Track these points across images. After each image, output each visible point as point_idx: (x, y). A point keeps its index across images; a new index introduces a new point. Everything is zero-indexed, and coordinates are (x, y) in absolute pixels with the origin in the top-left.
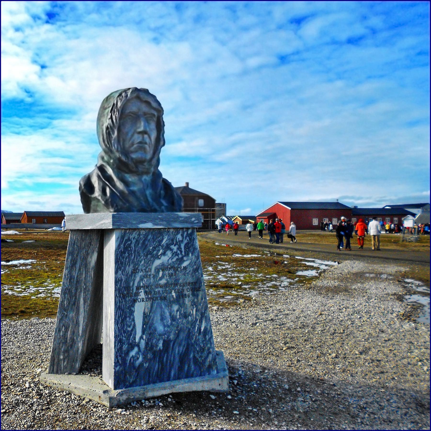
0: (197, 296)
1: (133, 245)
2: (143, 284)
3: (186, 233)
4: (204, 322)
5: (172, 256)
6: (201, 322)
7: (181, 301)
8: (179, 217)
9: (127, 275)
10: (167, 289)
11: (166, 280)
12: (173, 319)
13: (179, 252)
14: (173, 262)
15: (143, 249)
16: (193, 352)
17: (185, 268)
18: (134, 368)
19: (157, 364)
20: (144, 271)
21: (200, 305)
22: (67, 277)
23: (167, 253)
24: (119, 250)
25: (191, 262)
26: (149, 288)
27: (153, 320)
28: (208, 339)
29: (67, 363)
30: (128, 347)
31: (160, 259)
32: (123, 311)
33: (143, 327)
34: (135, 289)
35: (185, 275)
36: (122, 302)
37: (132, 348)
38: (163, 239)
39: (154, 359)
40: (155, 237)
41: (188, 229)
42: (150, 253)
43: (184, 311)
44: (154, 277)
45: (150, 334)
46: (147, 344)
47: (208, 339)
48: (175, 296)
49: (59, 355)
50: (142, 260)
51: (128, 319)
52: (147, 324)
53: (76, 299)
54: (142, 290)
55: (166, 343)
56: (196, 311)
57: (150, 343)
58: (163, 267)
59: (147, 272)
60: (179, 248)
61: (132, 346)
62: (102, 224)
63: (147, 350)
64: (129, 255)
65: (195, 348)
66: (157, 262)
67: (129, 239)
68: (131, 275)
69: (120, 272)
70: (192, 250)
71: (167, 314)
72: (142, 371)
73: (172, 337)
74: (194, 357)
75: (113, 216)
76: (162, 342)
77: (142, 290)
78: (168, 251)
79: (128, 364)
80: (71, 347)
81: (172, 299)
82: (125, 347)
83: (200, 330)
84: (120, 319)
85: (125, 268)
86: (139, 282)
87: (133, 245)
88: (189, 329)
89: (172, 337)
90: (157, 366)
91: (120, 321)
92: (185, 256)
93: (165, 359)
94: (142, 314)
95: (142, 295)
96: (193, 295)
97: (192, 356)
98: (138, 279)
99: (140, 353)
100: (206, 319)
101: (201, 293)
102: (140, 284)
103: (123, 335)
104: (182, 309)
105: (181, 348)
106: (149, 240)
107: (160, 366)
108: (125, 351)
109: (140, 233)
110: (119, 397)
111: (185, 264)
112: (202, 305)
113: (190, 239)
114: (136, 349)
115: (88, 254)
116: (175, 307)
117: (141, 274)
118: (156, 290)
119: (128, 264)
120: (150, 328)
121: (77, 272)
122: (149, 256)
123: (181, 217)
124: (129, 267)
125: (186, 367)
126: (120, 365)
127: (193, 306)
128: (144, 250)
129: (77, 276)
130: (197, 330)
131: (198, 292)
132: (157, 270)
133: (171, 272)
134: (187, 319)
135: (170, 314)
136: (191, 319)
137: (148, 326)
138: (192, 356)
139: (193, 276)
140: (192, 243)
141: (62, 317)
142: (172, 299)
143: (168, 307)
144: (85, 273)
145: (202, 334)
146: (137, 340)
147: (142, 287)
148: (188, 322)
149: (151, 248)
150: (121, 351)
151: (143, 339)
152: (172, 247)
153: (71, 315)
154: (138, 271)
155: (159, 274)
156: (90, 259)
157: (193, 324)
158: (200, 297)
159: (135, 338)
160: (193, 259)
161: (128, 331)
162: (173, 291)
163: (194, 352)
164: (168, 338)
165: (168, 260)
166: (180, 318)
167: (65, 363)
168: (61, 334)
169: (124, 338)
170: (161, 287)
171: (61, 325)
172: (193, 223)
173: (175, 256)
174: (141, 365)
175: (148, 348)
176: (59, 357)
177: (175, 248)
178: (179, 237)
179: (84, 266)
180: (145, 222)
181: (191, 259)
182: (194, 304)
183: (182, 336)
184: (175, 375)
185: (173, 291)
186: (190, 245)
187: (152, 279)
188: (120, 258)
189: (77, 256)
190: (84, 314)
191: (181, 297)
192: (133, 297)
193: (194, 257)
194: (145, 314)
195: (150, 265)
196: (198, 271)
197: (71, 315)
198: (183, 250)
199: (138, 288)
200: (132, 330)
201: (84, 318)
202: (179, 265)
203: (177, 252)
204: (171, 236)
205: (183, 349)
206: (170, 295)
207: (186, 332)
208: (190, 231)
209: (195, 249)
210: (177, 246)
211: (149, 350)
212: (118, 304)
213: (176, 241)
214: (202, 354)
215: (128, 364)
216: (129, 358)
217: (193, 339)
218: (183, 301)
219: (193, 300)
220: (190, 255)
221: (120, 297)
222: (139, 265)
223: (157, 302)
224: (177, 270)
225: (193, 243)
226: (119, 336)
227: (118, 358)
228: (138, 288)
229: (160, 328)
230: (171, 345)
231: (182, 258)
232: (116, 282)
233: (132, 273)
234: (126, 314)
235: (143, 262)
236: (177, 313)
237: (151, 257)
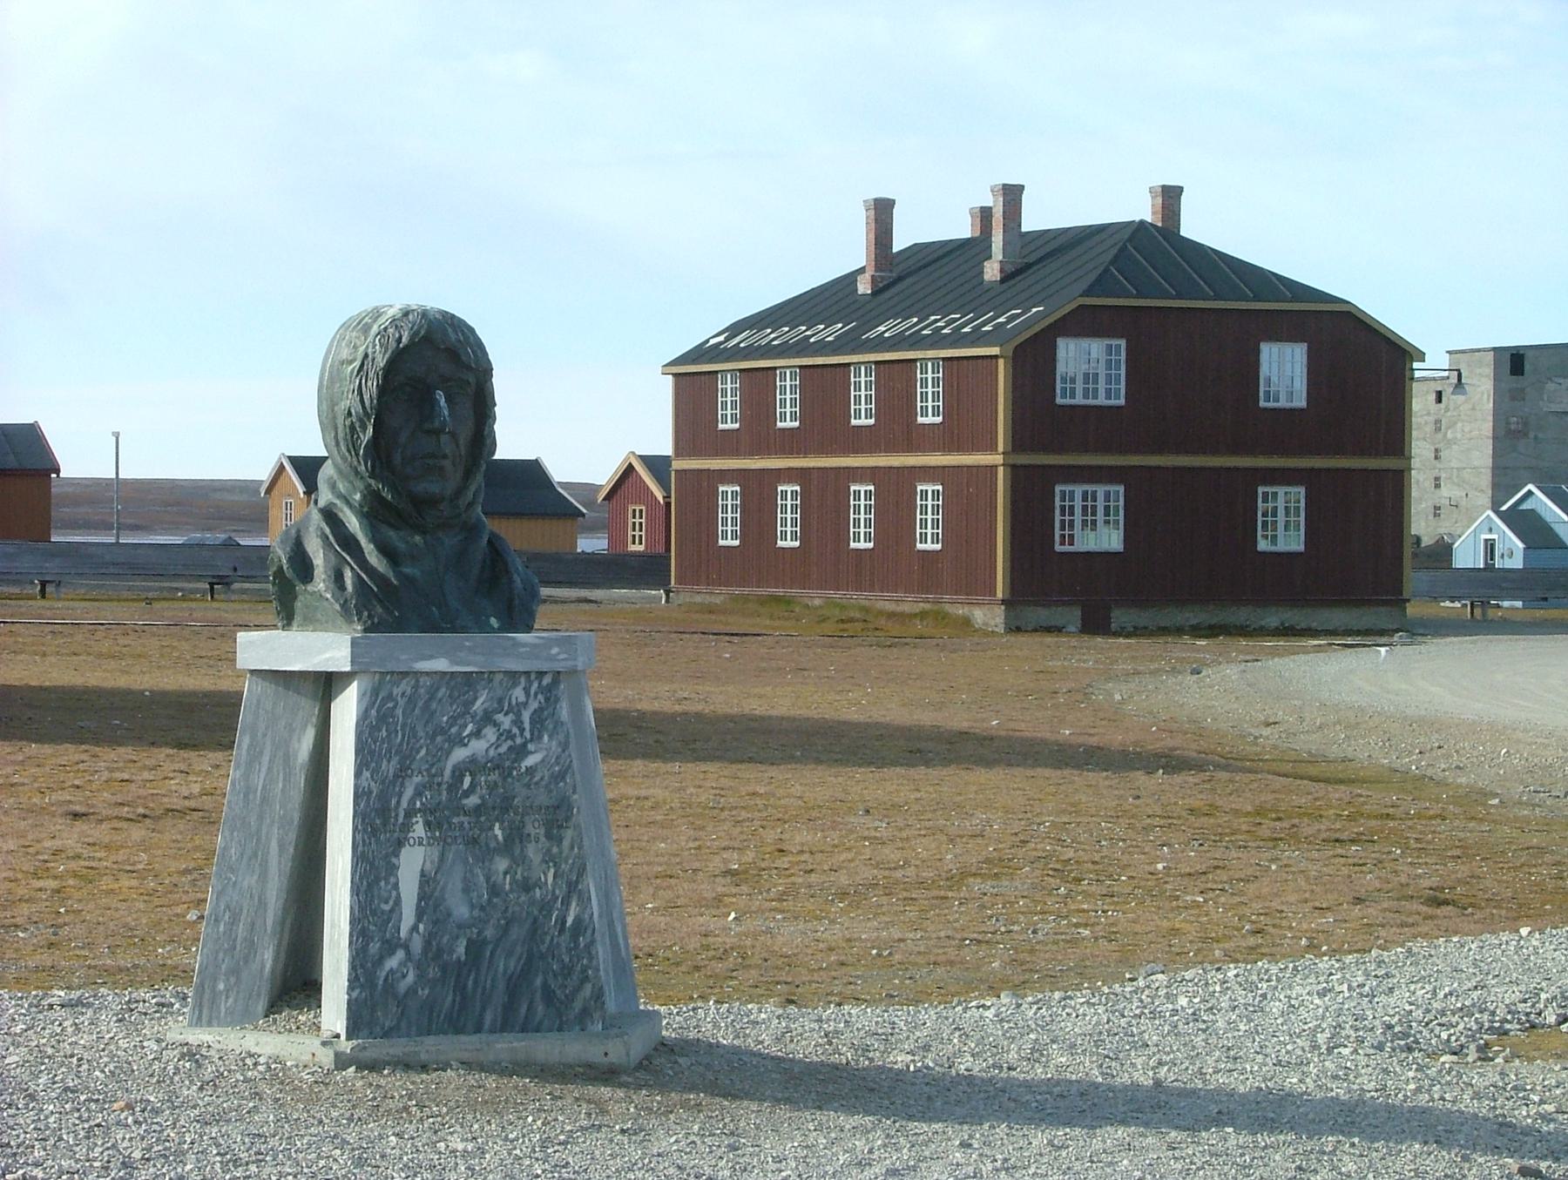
0: (561, 840)
1: (399, 712)
3: (535, 685)
4: (574, 904)
6: (566, 903)
7: (517, 852)
8: (516, 644)
9: (383, 782)
12: (494, 890)
13: (515, 730)
17: (531, 771)
27: (443, 889)
32: (372, 864)
34: (402, 814)
37: (392, 953)
38: (476, 699)
41: (541, 674)
44: (449, 790)
45: (435, 923)
46: (427, 944)
48: (500, 838)
49: (215, 980)
54: (419, 818)
55: (475, 947)
58: (472, 766)
60: (518, 722)
61: (390, 947)
66: (460, 754)
67: (390, 697)
69: (367, 774)
73: (489, 933)
74: (545, 985)
75: (354, 643)
77: (419, 818)
80: (246, 962)
81: (493, 845)
82: (374, 947)
83: (564, 922)
86: (412, 801)
87: (399, 712)
88: (535, 920)
89: (489, 933)
90: (450, 998)
92: (532, 740)
93: (470, 983)
95: (419, 830)
96: (549, 836)
97: (538, 982)
98: (409, 792)
101: (569, 834)
105: (512, 964)
111: (530, 761)
113: (547, 700)
114: (400, 954)
116: (502, 864)
120: (436, 907)
121: (262, 775)
122: (439, 739)
123: (525, 645)
125: (523, 1010)
126: (362, 986)
129: (264, 787)
133: (494, 777)
135: (488, 880)
138: (538, 982)
142: (493, 845)
146: (403, 934)
147: (420, 810)
152: (500, 717)
153: (246, 883)
157: (546, 907)
158: (566, 843)
161: (383, 912)
164: (479, 934)
166: (511, 890)
168: (222, 928)
169: (372, 928)
172: (552, 659)
174: (412, 991)
176: (214, 987)
177: (506, 721)
178: (518, 694)
180: (431, 657)
182: (549, 859)
183: (517, 932)
184: (494, 1021)
189: (265, 735)
196: (563, 779)
197: (246, 883)
198: (527, 725)
199: (410, 814)
200: (392, 911)
202: (515, 761)
204: (499, 693)
207: (527, 926)
208: (547, 680)
209: (558, 724)
216: (384, 974)
219: (549, 850)
220: (546, 738)
221: (365, 830)
223: (454, 847)
224: (510, 774)
228: (410, 814)
229: (461, 911)
231: (524, 745)
232: (357, 796)
233: (396, 776)
235: (423, 752)
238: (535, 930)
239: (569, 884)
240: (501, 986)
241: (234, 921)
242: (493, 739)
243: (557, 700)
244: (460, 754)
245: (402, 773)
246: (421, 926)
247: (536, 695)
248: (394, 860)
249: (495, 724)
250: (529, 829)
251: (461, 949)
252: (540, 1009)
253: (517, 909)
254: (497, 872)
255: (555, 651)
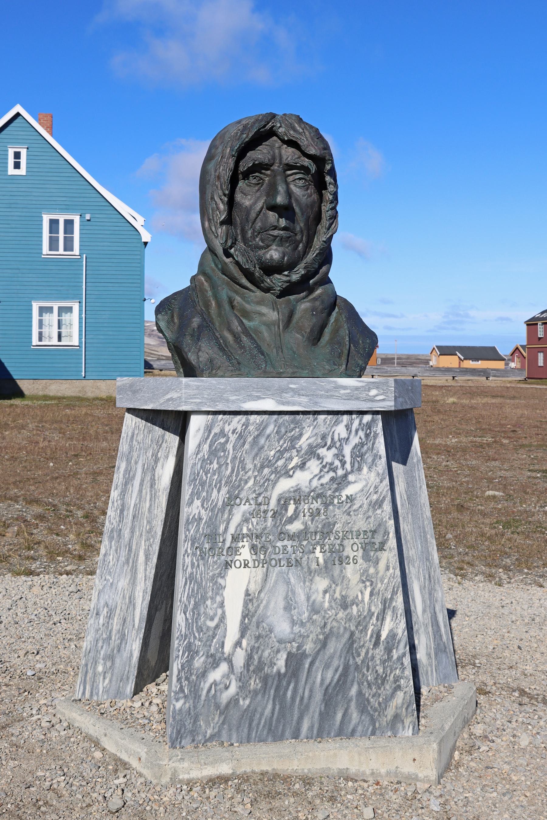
0: (377, 562)
1: (230, 446)
2: (249, 530)
4: (388, 618)
5: (321, 471)
6: (381, 618)
8: (339, 387)
10: (305, 543)
11: (303, 523)
13: (337, 463)
14: (322, 485)
15: (254, 453)
16: (359, 684)
17: (351, 499)
18: (217, 706)
19: (271, 702)
20: (252, 502)
21: (382, 582)
22: (115, 504)
23: (308, 464)
24: (199, 456)
25: (366, 486)
26: (264, 539)
27: (266, 607)
28: (395, 657)
29: (110, 681)
30: (205, 662)
31: (291, 476)
33: (242, 622)
35: (349, 514)
36: (198, 566)
37: (215, 665)
38: (301, 435)
39: (265, 692)
40: (283, 430)
41: (362, 413)
42: (267, 463)
43: (341, 592)
44: (274, 516)
45: (258, 638)
46: (249, 658)
47: (395, 657)
48: (321, 561)
49: (96, 663)
50: (249, 478)
51: (209, 602)
52: (253, 616)
53: (130, 550)
55: (295, 661)
56: (371, 594)
57: (256, 657)
58: (297, 496)
59: (260, 504)
60: (340, 456)
61: (214, 661)
62: (169, 400)
63: (248, 670)
64: (220, 466)
65: (364, 675)
66: (284, 485)
67: (222, 433)
68: (222, 510)
70: (370, 460)
71: (301, 597)
72: (235, 715)
73: (309, 647)
74: (360, 693)
76: (285, 657)
78: (312, 460)
79: (203, 697)
80: (119, 651)
81: (314, 566)
83: (379, 636)
84: (192, 602)
85: (209, 494)
88: (352, 634)
89: (309, 647)
90: (270, 706)
91: (191, 606)
92: (352, 471)
93: (289, 693)
94: (243, 595)
95: (245, 553)
96: (366, 558)
97: (354, 691)
99: (232, 677)
100: (393, 611)
102: (241, 529)
103: (197, 635)
104: (338, 589)
105: (329, 674)
106: (269, 436)
107: (277, 707)
108: (198, 669)
109: (247, 420)
110: (174, 765)
111: (349, 491)
112: (386, 581)
113: (367, 436)
114: (224, 667)
115: (157, 461)
116: (321, 583)
117: (244, 508)
118: (279, 544)
119: (216, 486)
122: (266, 471)
123: (345, 388)
124: (219, 492)
125: (339, 716)
126: (185, 697)
127: (364, 582)
128: (256, 455)
130: (372, 636)
131: (379, 553)
132: (283, 502)
133: (315, 505)
134: (349, 610)
135: (308, 599)
136: (359, 611)
137: (254, 620)
138: (354, 691)
139: (369, 517)
140: (370, 445)
141: (104, 587)
143: (304, 582)
144: (151, 500)
145: (382, 647)
146: (228, 648)
147: (248, 535)
148: (349, 619)
149: (272, 453)
150: (190, 670)
151: (240, 647)
152: (322, 451)
154: (238, 501)
155: (286, 510)
156: (161, 471)
157: (362, 623)
158: (382, 565)
159: (223, 643)
160: (372, 479)
161: (208, 628)
162: (318, 548)
163: (360, 684)
164: (299, 648)
165: (310, 481)
167: (107, 681)
169: (197, 643)
170: (291, 537)
171: (102, 603)
172: (372, 400)
173: (328, 472)
174: (234, 701)
175: (252, 668)
176: (95, 668)
177: (328, 455)
178: (341, 430)
179: (149, 485)
180: (259, 398)
181: (365, 480)
182: (366, 579)
184: (311, 728)
185: (318, 548)
186: (365, 447)
187: (270, 520)
188: (199, 473)
189: (136, 463)
190: (145, 584)
191: (337, 562)
192: (223, 558)
193: (373, 475)
194: (250, 595)
195: (266, 490)
196: (380, 506)
198: (348, 459)
199: (235, 538)
200: (217, 627)
201: (145, 592)
202: (336, 490)
203: (332, 464)
204: (323, 429)
205: (334, 675)
206: (311, 556)
207: (344, 640)
210: (334, 451)
211: (254, 671)
212: (189, 569)
213: (333, 439)
214: (380, 688)
215: (203, 697)
216: (207, 685)
217: (359, 655)
218: (342, 571)
219: (366, 571)
220: (365, 469)
221: (194, 554)
222: (242, 489)
223: (278, 569)
224: (332, 503)
225: (373, 444)
226: (186, 636)
227: (181, 683)
229: (283, 627)
230: (307, 666)
231: (345, 476)
233: (225, 504)
234: (206, 593)
235: (251, 483)
236: (324, 598)
237: (272, 473)
238: (351, 645)
239: (384, 602)
240: (318, 696)
241: (109, 617)
242: (316, 471)
243: (376, 436)
244: (284, 485)
245: (231, 502)
246: (244, 643)
247: (357, 431)
248: (220, 581)
249: (319, 458)
250: (348, 551)
251: (281, 663)
252: (355, 716)
253: (335, 624)
254: (317, 591)
255: (373, 392)
